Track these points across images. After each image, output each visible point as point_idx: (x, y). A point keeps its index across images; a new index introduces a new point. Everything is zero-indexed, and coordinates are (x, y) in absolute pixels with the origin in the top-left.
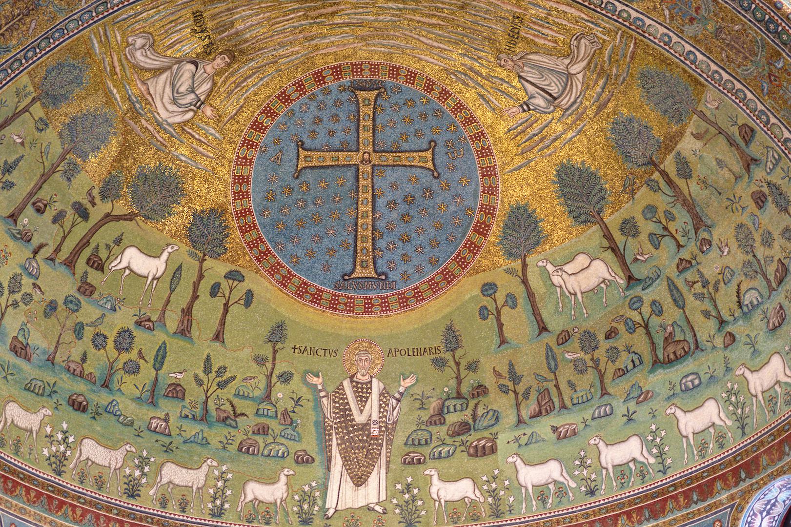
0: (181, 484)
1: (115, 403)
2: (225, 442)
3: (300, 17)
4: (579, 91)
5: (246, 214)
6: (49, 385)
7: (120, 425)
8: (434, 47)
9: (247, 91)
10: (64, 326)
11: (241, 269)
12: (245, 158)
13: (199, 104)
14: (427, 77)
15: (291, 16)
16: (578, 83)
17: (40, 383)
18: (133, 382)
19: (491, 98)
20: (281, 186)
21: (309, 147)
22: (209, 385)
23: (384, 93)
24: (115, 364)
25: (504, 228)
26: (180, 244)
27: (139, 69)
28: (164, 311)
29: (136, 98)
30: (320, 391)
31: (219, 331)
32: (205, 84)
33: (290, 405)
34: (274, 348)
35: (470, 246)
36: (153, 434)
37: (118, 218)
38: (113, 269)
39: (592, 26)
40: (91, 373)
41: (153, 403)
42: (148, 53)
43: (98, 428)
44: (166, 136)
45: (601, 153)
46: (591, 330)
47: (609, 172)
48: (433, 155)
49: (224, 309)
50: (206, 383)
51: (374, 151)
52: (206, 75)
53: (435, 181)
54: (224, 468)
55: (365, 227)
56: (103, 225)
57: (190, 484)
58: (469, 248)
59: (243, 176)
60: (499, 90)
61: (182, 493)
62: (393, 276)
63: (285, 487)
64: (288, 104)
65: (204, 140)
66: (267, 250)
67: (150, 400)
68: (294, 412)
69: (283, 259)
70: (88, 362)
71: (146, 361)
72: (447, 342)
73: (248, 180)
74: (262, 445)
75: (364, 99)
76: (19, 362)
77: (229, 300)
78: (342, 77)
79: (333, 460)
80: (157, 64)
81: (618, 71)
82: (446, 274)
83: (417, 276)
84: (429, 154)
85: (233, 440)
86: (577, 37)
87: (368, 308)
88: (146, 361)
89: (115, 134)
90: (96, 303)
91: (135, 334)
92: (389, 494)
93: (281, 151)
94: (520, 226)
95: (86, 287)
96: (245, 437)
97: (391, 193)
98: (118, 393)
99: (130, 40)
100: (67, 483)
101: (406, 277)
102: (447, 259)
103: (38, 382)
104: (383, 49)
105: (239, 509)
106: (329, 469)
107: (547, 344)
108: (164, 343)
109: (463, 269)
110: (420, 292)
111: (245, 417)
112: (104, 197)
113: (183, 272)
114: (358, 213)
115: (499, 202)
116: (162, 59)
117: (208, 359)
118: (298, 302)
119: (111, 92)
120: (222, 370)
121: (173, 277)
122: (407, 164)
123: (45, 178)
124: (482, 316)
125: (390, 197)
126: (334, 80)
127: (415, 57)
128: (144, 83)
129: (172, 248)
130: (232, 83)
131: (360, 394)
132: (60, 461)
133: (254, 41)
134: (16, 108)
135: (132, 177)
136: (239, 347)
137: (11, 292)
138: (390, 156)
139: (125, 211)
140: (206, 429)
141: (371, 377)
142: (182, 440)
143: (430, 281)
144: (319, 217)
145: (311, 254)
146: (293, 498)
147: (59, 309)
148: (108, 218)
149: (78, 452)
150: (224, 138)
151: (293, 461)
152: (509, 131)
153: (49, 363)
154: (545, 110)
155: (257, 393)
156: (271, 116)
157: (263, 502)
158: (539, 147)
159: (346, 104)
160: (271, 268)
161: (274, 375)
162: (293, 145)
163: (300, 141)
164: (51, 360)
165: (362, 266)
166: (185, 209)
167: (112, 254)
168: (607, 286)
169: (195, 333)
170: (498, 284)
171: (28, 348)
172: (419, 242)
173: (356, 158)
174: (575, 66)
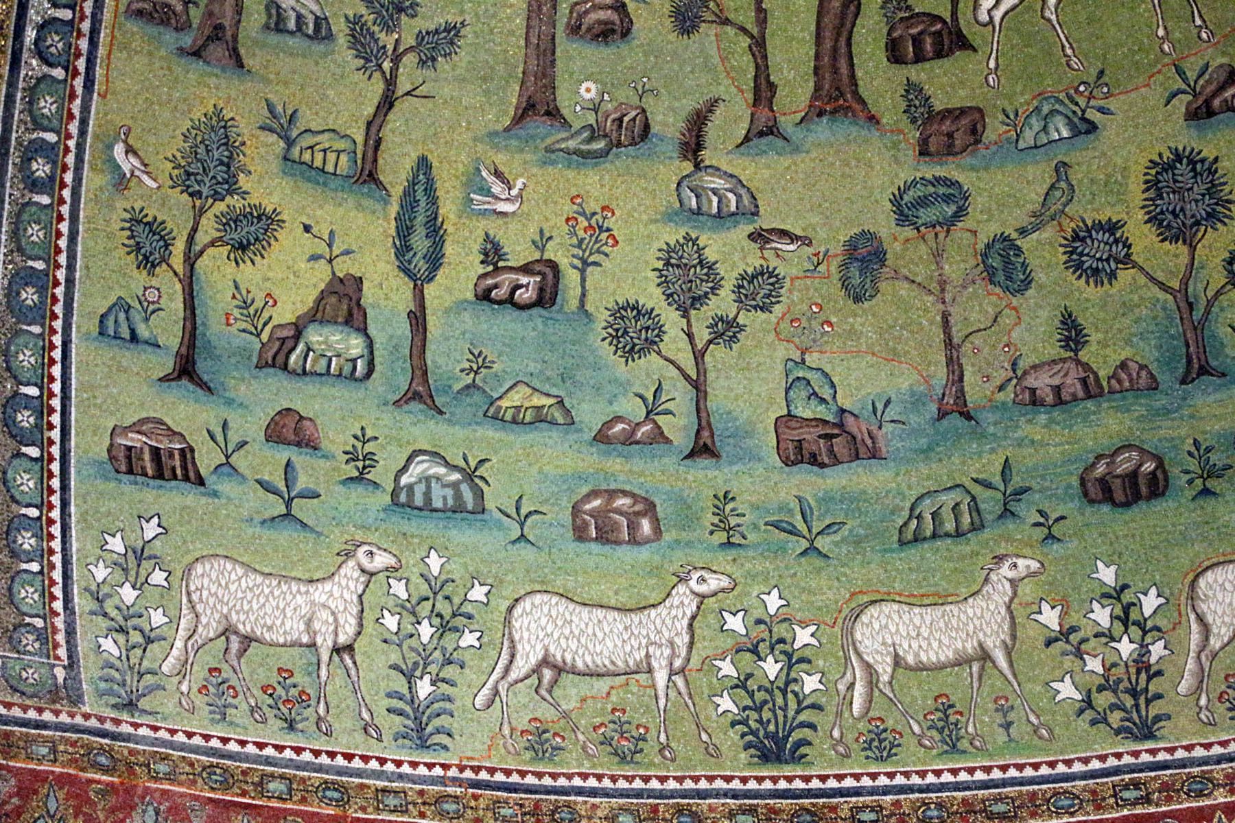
6: (987, 485)
10: (943, 284)
40: (1123, 365)
70: (1094, 337)
76: (837, 479)
90: (1013, 147)
91: (1208, 153)
95: (947, 126)
100: (1189, 748)
103: (943, 498)
132: (1134, 693)
137: (688, 304)
147: (893, 249)
149: (1195, 627)
153: (955, 420)
171: (849, 420)
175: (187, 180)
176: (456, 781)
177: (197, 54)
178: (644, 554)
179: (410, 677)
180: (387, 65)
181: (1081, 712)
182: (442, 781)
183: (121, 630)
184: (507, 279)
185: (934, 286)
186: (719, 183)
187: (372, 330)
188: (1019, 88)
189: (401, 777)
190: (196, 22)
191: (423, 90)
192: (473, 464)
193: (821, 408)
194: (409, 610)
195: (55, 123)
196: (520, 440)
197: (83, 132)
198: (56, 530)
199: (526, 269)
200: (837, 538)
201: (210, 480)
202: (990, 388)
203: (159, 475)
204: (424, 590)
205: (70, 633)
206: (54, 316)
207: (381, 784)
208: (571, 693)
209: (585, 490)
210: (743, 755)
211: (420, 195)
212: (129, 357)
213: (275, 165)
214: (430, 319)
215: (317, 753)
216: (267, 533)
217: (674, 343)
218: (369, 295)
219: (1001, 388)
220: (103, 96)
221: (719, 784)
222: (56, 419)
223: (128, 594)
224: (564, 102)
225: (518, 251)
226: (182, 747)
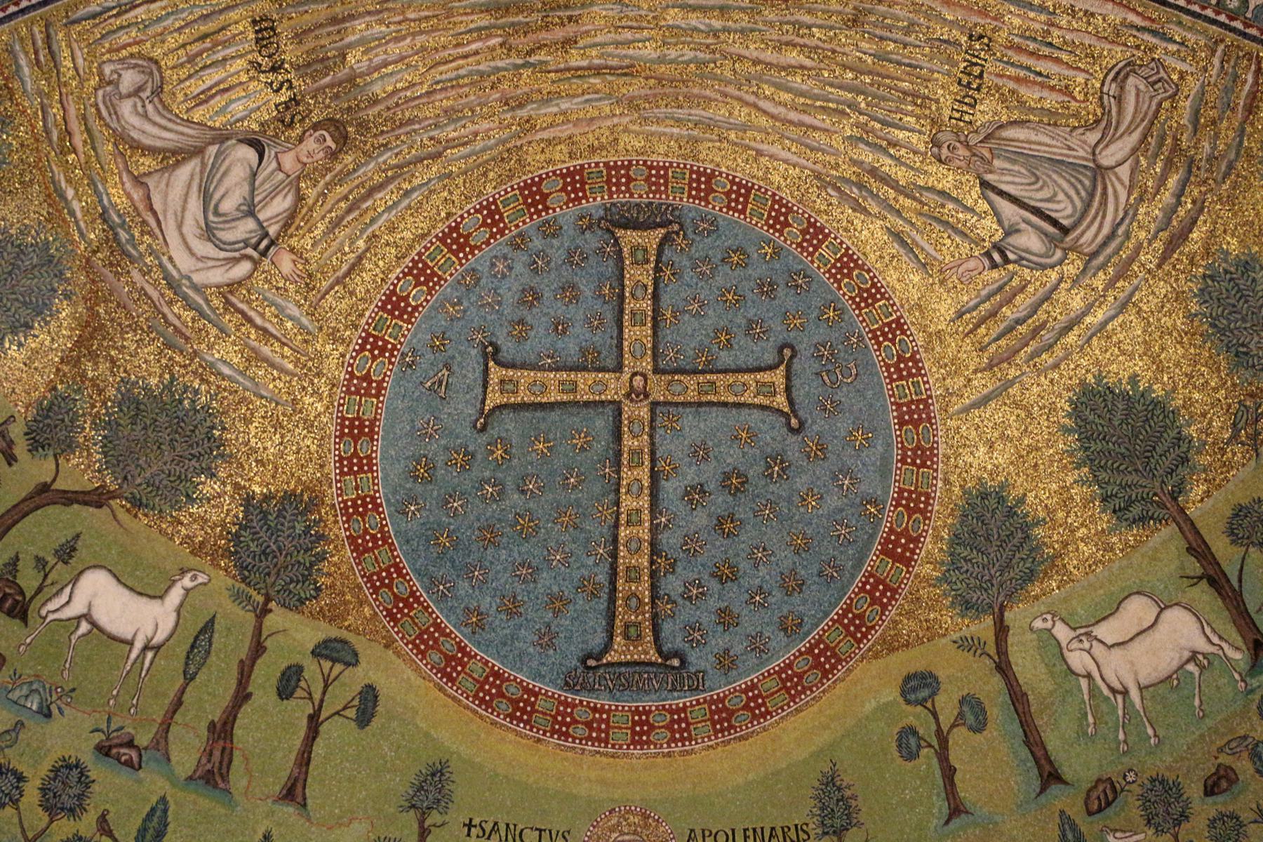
3: (492, 49)
4: (1122, 207)
5: (366, 510)
8: (791, 122)
9: (373, 221)
11: (350, 637)
12: (367, 378)
13: (264, 245)
14: (774, 195)
15: (474, 46)
16: (1119, 187)
19: (918, 238)
20: (446, 448)
21: (509, 357)
23: (677, 234)
25: (951, 544)
26: (213, 573)
27: (128, 145)
28: (166, 726)
29: (120, 216)
31: (296, 780)
32: (279, 199)
34: (421, 823)
35: (875, 588)
37: (69, 498)
38: (51, 617)
39: (1155, 41)
42: (150, 107)
44: (188, 315)
45: (1174, 352)
46: (1167, 774)
47: (1196, 396)
48: (788, 378)
49: (309, 728)
51: (656, 371)
53: (792, 439)
55: (634, 546)
58: (871, 593)
59: (362, 422)
60: (936, 219)
62: (699, 660)
64: (466, 257)
65: (275, 332)
66: (413, 594)
69: (447, 617)
72: (826, 813)
73: (372, 432)
75: (635, 249)
77: (321, 706)
78: (585, 197)
80: (167, 138)
81: (1214, 148)
82: (819, 655)
83: (752, 660)
84: (778, 377)
86: (1118, 73)
87: (642, 733)
89: (67, 296)
91: (93, 775)
93: (448, 366)
94: (988, 539)
97: (694, 468)
99: (107, 70)
101: (726, 662)
104: (676, 130)
107: (1062, 812)
108: (163, 800)
109: (859, 641)
110: (760, 695)
113: (216, 636)
114: (618, 514)
115: (940, 484)
116: (180, 128)
118: (481, 717)
119: (62, 196)
121: (193, 647)
122: (731, 399)
124: (904, 752)
125: (691, 475)
126: (566, 204)
127: (750, 148)
128: (138, 181)
129: (194, 578)
130: (339, 201)
135: (104, 403)
136: (340, 818)
138: (691, 382)
143: (782, 670)
145: (512, 608)
148: (44, 495)
150: (321, 329)
152: (960, 315)
154: (1043, 261)
156: (426, 283)
158: (1029, 349)
159: (593, 260)
160: (420, 636)
162: (474, 352)
163: (491, 344)
165: (626, 636)
166: (228, 488)
167: (49, 581)
168: (1202, 668)
169: (238, 779)
170: (941, 675)
172: (757, 582)
173: (614, 387)
174: (1112, 148)
188: (31, 664)
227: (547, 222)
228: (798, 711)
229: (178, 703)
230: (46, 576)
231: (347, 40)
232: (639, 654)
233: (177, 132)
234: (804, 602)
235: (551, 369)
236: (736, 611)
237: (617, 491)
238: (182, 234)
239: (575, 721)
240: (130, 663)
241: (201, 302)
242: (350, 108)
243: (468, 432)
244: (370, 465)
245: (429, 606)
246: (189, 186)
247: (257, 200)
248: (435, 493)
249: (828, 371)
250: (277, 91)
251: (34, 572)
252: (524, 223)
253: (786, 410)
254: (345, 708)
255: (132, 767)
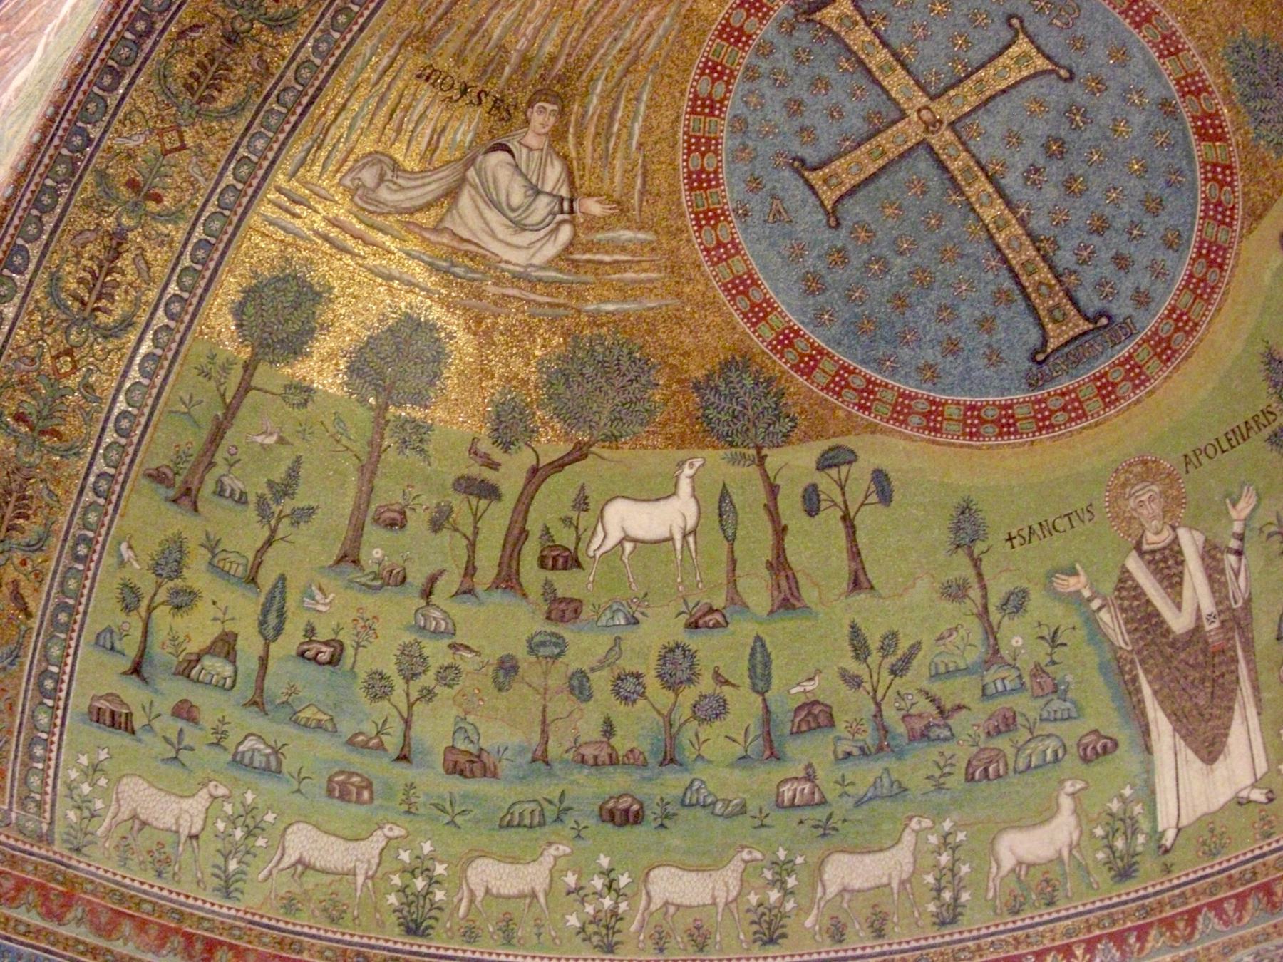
0: (866, 885)
1: (696, 785)
2: (937, 773)
6: (550, 802)
7: (720, 820)
9: (630, 135)
10: (546, 690)
12: (720, 244)
17: (533, 806)
18: (724, 734)
20: (819, 257)
22: (875, 678)
24: (675, 716)
28: (732, 582)
29: (446, 260)
30: (1090, 600)
31: (856, 572)
32: (549, 169)
33: (1041, 652)
34: (971, 555)
36: (791, 812)
37: (559, 465)
38: (598, 554)
40: (632, 751)
41: (775, 754)
42: (400, 181)
43: (677, 842)
50: (866, 677)
52: (537, 154)
53: (1072, 87)
54: (947, 825)
55: (1015, 244)
56: (536, 490)
57: (885, 880)
58: (1214, 179)
61: (872, 902)
62: (1121, 308)
63: (1072, 820)
66: (869, 381)
67: (768, 753)
68: (1053, 663)
69: (907, 384)
71: (733, 685)
74: (1010, 752)
77: (846, 507)
79: (1152, 727)
80: (433, 188)
83: (1160, 286)
84: (1023, 45)
85: (953, 765)
88: (733, 685)
91: (693, 647)
92: (1271, 756)
94: (1266, 84)
95: (562, 606)
96: (975, 750)
98: (699, 763)
101: (1142, 299)
102: (1193, 224)
103: (526, 805)
105: (991, 895)
106: (1148, 749)
108: (758, 638)
109: (1230, 225)
110: (1182, 315)
111: (964, 712)
112: (507, 446)
113: (735, 498)
114: (986, 226)
117: (855, 631)
118: (979, 448)
120: (890, 640)
121: (721, 515)
122: (1003, 85)
123: (369, 469)
125: (1020, 161)
128: (435, 230)
129: (692, 465)
131: (1166, 571)
132: (607, 927)
133: (566, 51)
134: (223, 396)
137: (410, 677)
139: (563, 448)
140: (892, 764)
141: (1174, 528)
142: (851, 801)
143: (1188, 282)
144: (924, 272)
145: (952, 348)
146: (1092, 835)
147: (523, 666)
148: (537, 475)
149: (644, 897)
150: (656, 232)
151: (1078, 762)
153: (540, 764)
155: (974, 655)
156: (708, 150)
157: (1034, 865)
159: (816, 49)
160: (894, 411)
161: (992, 608)
163: (794, 159)
164: (541, 758)
165: (1055, 321)
167: (580, 532)
169: (809, 594)
171: (484, 756)
172: (1126, 219)
173: (911, 130)
175: (156, 568)
176: (242, 919)
177: (175, 501)
178: (362, 810)
179: (226, 858)
180: (273, 522)
181: (579, 933)
182: (235, 918)
183: (79, 808)
184: (315, 647)
185: (542, 690)
186: (437, 614)
187: (238, 663)
189: (213, 912)
190: (178, 484)
191: (290, 538)
192: (279, 745)
193: (471, 745)
194: (232, 821)
195: (94, 527)
196: (308, 735)
197: (107, 534)
198: (54, 747)
199: (326, 643)
200: (468, 817)
201: (139, 732)
202: (561, 750)
203: (113, 725)
204: (241, 811)
205: (53, 805)
206: (73, 631)
207: (202, 914)
208: (311, 880)
209: (337, 769)
210: (397, 930)
211: (277, 593)
212: (107, 658)
213: (203, 567)
214: (271, 662)
215: (171, 892)
216: (163, 767)
217: (398, 696)
218: (240, 644)
219: (567, 751)
220: (122, 516)
221: (382, 943)
222: (64, 686)
223: (86, 788)
224: (363, 557)
225: (324, 633)
226: (101, 877)
227: (759, 45)
228: (1218, 310)
229: (733, 561)
230: (577, 528)
231: (495, 36)
232: (1072, 329)
233: (434, 181)
234: (1171, 214)
235: (855, 148)
236: (1125, 252)
237: (973, 210)
238: (501, 241)
239: (1052, 412)
240: (678, 553)
241: (554, 274)
242: (541, 76)
243: (828, 233)
244: (770, 305)
245: (887, 384)
246: (477, 207)
247: (534, 181)
248: (836, 295)
249: (1057, 17)
250: (480, 103)
251: (565, 530)
252: (742, 57)
253: (1050, 67)
254: (866, 498)
255: (722, 626)
